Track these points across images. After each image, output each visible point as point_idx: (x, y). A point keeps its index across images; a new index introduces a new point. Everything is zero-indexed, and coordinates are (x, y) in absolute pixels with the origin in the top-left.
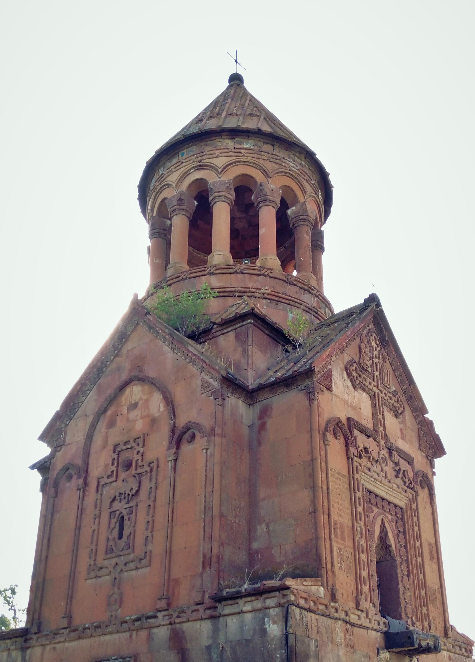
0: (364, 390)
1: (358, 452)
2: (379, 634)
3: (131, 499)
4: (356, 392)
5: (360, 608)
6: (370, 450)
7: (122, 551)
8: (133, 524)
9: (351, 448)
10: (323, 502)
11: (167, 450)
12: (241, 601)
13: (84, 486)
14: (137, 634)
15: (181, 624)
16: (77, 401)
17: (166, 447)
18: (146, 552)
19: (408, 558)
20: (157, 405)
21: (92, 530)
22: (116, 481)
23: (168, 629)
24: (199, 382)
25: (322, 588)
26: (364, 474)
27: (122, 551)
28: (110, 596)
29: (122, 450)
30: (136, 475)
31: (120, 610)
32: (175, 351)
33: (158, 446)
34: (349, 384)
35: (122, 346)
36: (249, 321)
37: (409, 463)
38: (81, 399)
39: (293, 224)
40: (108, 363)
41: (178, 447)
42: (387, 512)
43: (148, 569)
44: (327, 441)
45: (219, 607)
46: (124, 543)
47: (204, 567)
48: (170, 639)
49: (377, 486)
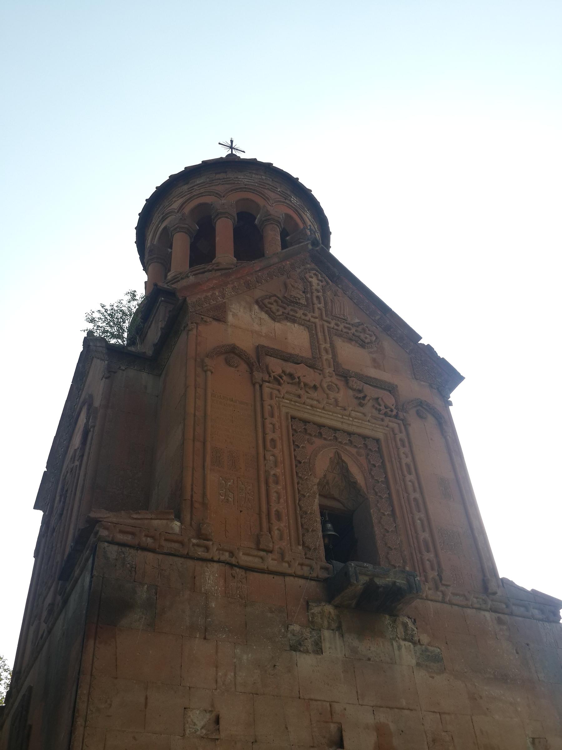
0: (294, 321)
1: (270, 376)
2: (313, 583)
4: (277, 325)
5: (261, 547)
6: (296, 376)
9: (255, 373)
10: (194, 430)
19: (390, 494)
25: (178, 524)
26: (288, 401)
34: (264, 316)
37: (390, 391)
42: (346, 444)
44: (207, 366)
49: (318, 414)
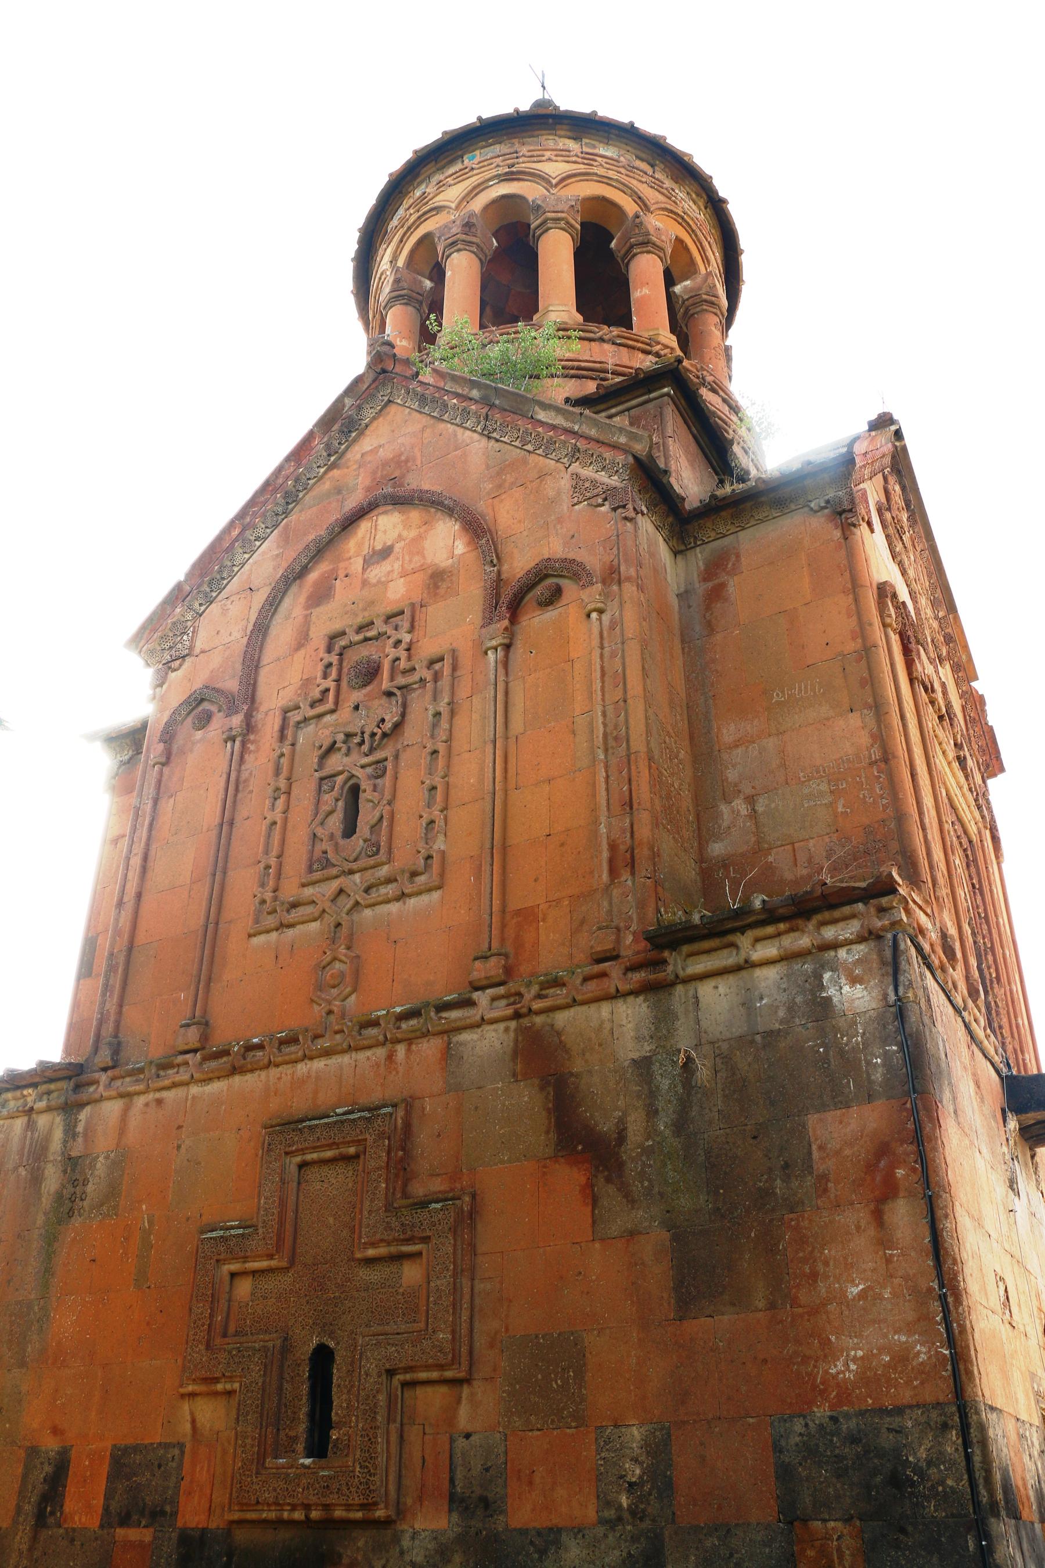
3: (379, 745)
7: (355, 860)
8: (387, 796)
11: (483, 626)
12: (744, 941)
13: (245, 731)
14: (409, 1050)
15: (551, 1014)
16: (229, 564)
17: (479, 622)
18: (429, 857)
20: (445, 542)
21: (267, 822)
22: (333, 711)
23: (507, 1029)
24: (565, 483)
27: (355, 860)
28: (324, 968)
29: (351, 644)
30: (396, 691)
31: (353, 997)
32: (494, 435)
33: (456, 624)
35: (347, 448)
36: (666, 390)
38: (239, 558)
39: (687, 310)
40: (311, 482)
41: (514, 619)
43: (436, 895)
45: (671, 961)
46: (361, 842)
47: (613, 872)
48: (515, 1053)
